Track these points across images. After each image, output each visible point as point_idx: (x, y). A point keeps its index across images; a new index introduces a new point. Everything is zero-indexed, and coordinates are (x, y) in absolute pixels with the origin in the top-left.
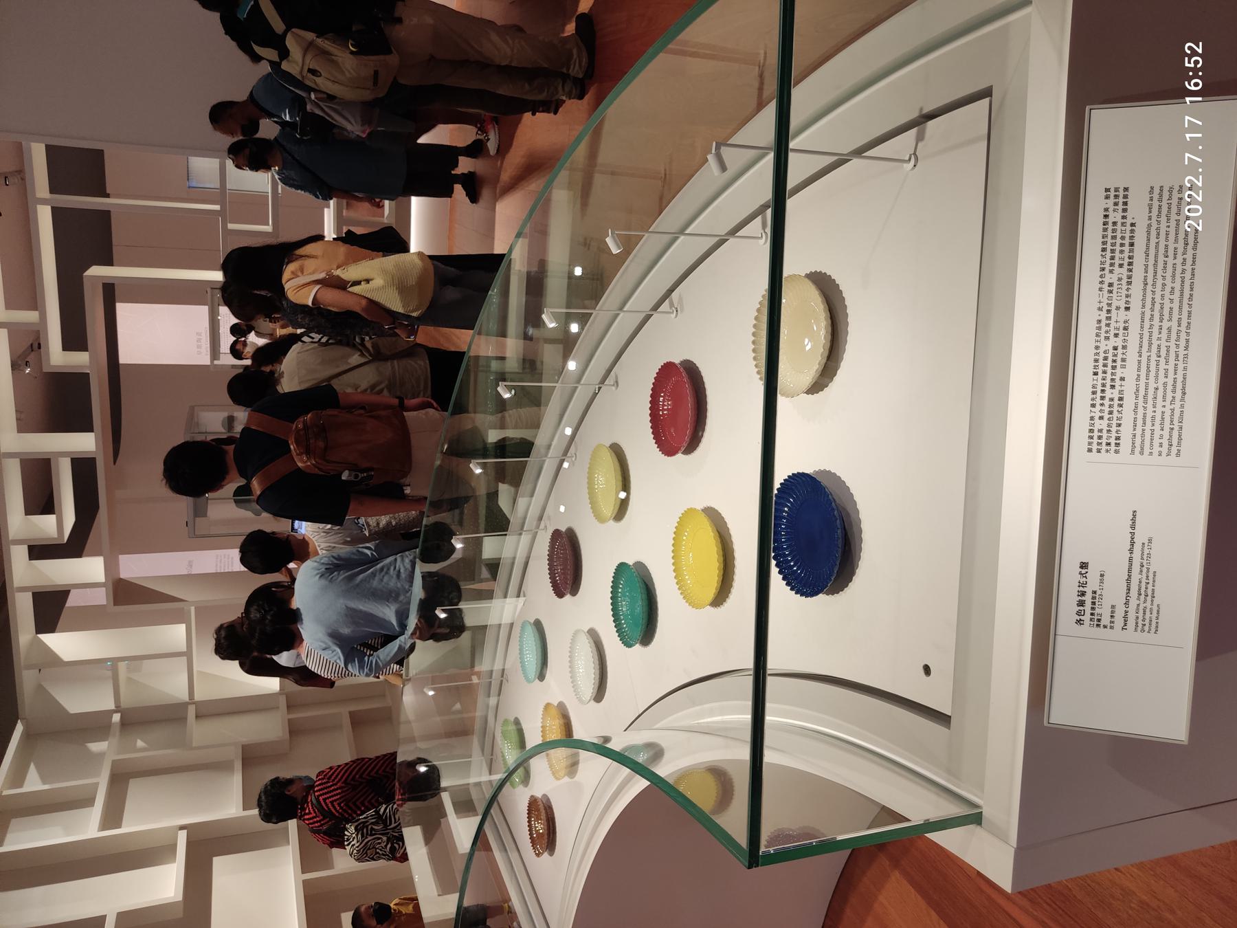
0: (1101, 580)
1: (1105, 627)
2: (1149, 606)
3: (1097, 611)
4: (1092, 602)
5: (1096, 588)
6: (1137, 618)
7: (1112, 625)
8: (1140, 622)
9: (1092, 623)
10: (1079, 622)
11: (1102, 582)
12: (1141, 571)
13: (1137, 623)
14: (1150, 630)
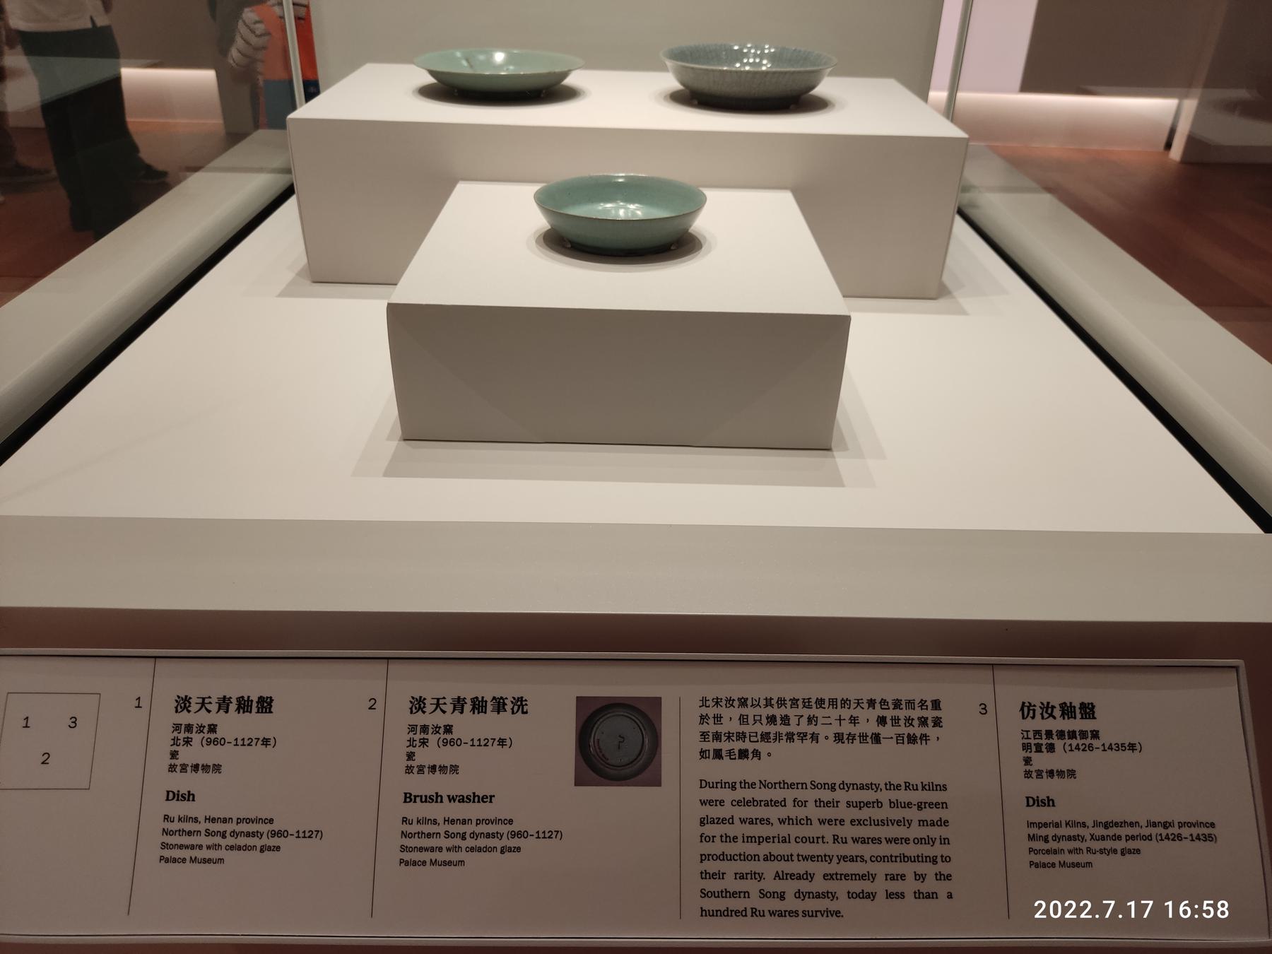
0: (1123, 745)
1: (1027, 761)
2: (1083, 846)
3: (1058, 744)
4: (1074, 732)
5: (1106, 738)
7: (1034, 775)
8: (1050, 832)
9: (1031, 735)
10: (1027, 710)
11: (1120, 747)
13: (1045, 825)
14: (1036, 852)
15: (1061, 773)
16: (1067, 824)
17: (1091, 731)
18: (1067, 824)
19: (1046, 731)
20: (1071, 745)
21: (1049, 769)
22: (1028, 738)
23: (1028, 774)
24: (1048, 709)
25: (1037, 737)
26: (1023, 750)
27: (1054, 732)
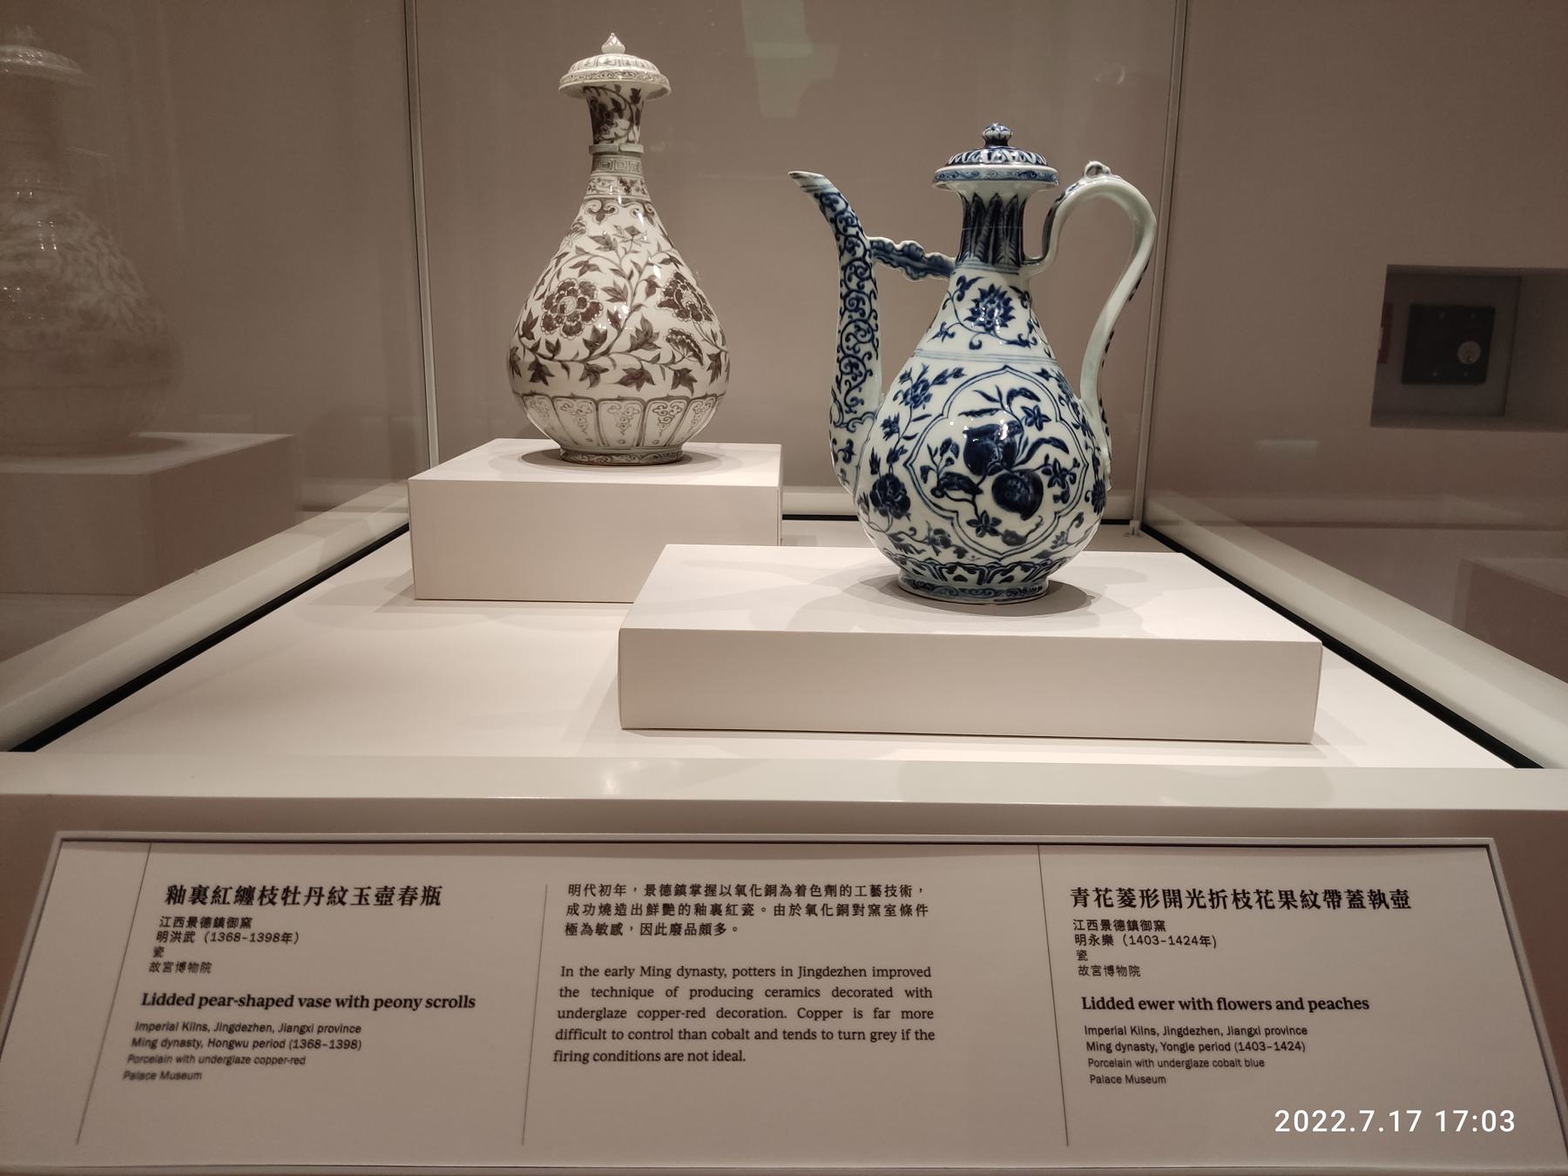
1: (158, 952)
3: (199, 931)
4: (222, 920)
5: (256, 927)
6: (172, 1027)
7: (161, 968)
9: (171, 922)
10: (175, 895)
12: (289, 1029)
15: (193, 967)
16: (185, 1026)
17: (243, 919)
18: (185, 1026)
19: (190, 918)
20: (214, 934)
21: (181, 961)
22: (167, 926)
23: (154, 967)
24: (199, 894)
25: (178, 924)
26: (158, 939)
27: (199, 920)
